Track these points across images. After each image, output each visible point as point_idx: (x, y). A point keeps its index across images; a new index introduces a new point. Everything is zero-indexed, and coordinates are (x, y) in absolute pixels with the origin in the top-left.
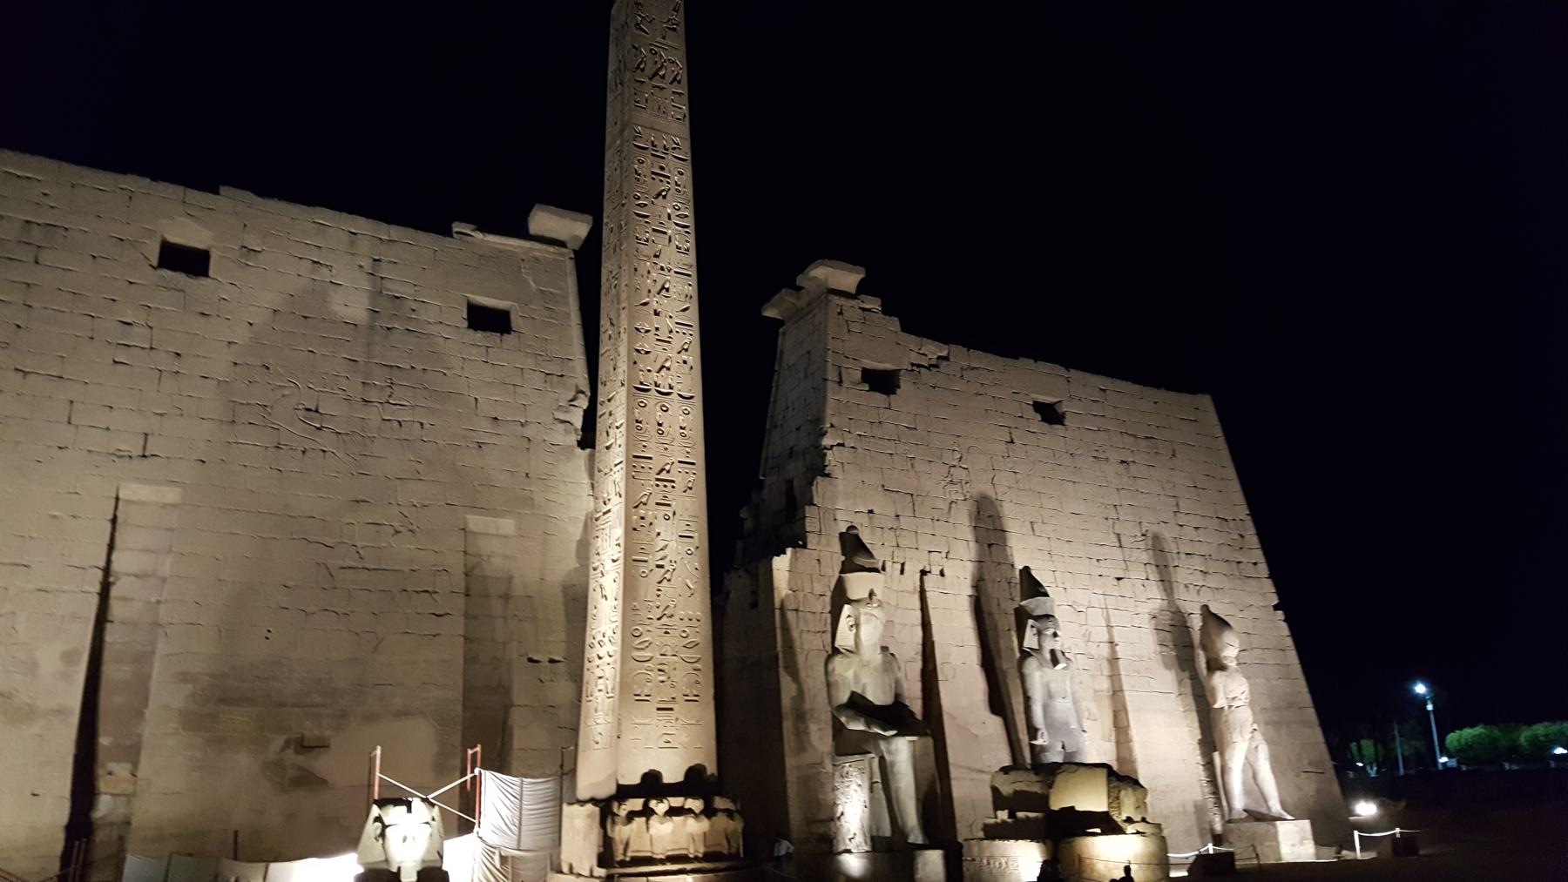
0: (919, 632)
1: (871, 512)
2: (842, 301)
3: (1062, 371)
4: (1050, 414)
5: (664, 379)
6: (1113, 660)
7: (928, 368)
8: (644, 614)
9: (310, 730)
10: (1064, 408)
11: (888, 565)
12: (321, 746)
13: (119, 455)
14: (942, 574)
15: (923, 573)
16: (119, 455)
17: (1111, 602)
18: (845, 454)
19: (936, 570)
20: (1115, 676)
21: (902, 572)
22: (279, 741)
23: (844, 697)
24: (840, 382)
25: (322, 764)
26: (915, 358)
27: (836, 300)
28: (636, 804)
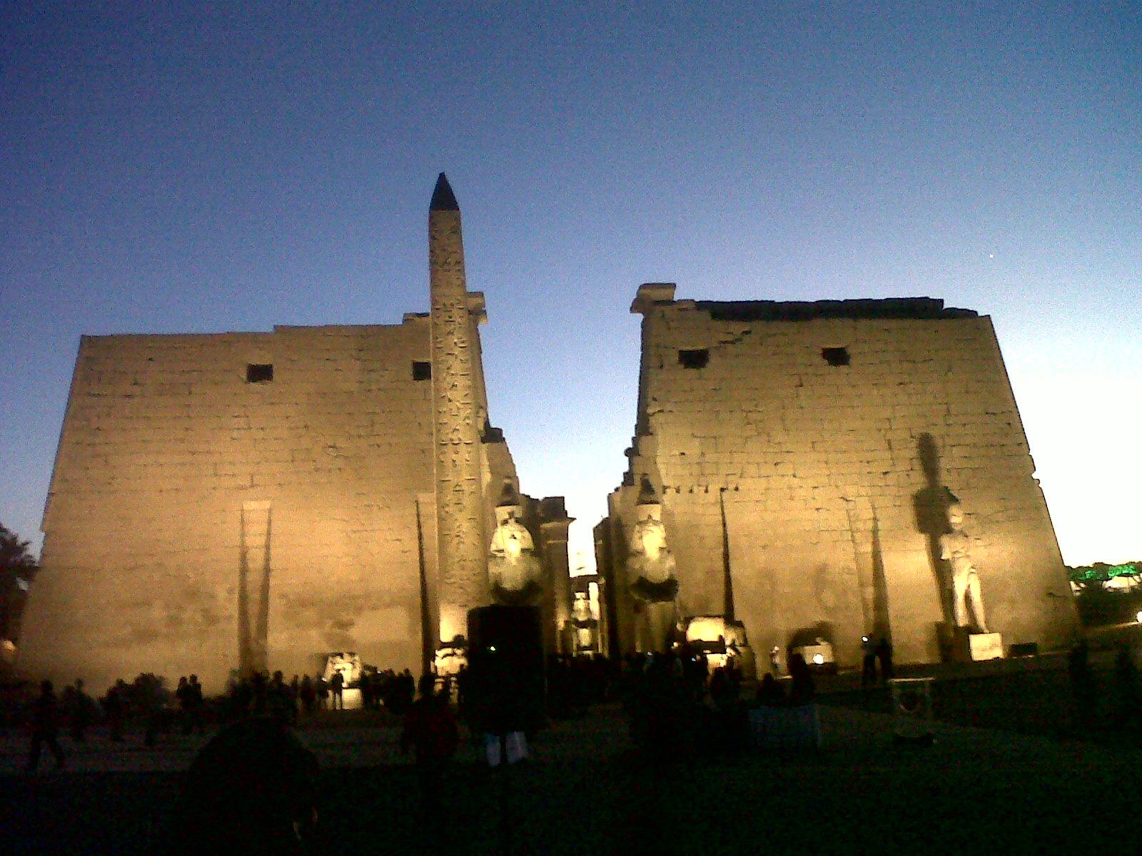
0: (720, 528)
1: (683, 454)
2: (663, 308)
3: (850, 322)
4: (837, 357)
5: (455, 437)
6: (875, 531)
7: (732, 343)
8: (450, 561)
9: (345, 617)
10: (849, 351)
11: (695, 489)
12: (351, 624)
13: (242, 488)
14: (737, 489)
15: (722, 490)
16: (242, 488)
17: (877, 491)
18: (660, 417)
19: (732, 487)
20: (876, 543)
21: (706, 491)
22: (329, 623)
23: (634, 580)
24: (661, 367)
25: (354, 633)
26: (723, 337)
27: (658, 308)
28: (449, 651)
